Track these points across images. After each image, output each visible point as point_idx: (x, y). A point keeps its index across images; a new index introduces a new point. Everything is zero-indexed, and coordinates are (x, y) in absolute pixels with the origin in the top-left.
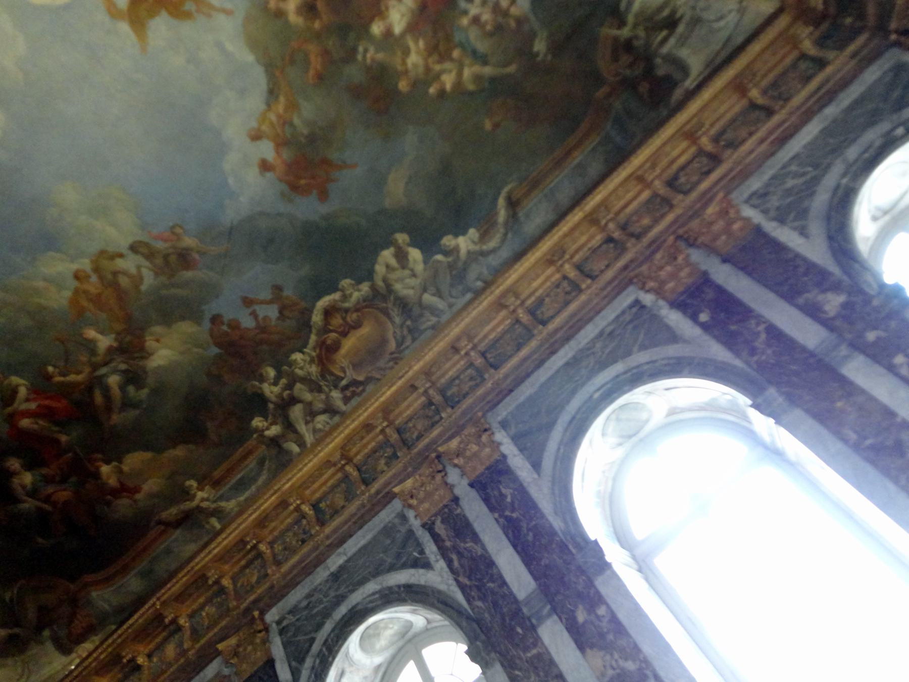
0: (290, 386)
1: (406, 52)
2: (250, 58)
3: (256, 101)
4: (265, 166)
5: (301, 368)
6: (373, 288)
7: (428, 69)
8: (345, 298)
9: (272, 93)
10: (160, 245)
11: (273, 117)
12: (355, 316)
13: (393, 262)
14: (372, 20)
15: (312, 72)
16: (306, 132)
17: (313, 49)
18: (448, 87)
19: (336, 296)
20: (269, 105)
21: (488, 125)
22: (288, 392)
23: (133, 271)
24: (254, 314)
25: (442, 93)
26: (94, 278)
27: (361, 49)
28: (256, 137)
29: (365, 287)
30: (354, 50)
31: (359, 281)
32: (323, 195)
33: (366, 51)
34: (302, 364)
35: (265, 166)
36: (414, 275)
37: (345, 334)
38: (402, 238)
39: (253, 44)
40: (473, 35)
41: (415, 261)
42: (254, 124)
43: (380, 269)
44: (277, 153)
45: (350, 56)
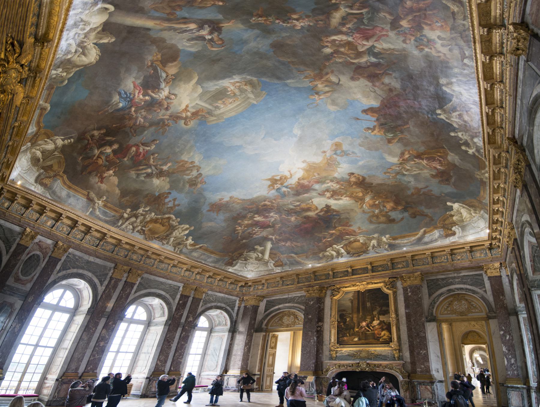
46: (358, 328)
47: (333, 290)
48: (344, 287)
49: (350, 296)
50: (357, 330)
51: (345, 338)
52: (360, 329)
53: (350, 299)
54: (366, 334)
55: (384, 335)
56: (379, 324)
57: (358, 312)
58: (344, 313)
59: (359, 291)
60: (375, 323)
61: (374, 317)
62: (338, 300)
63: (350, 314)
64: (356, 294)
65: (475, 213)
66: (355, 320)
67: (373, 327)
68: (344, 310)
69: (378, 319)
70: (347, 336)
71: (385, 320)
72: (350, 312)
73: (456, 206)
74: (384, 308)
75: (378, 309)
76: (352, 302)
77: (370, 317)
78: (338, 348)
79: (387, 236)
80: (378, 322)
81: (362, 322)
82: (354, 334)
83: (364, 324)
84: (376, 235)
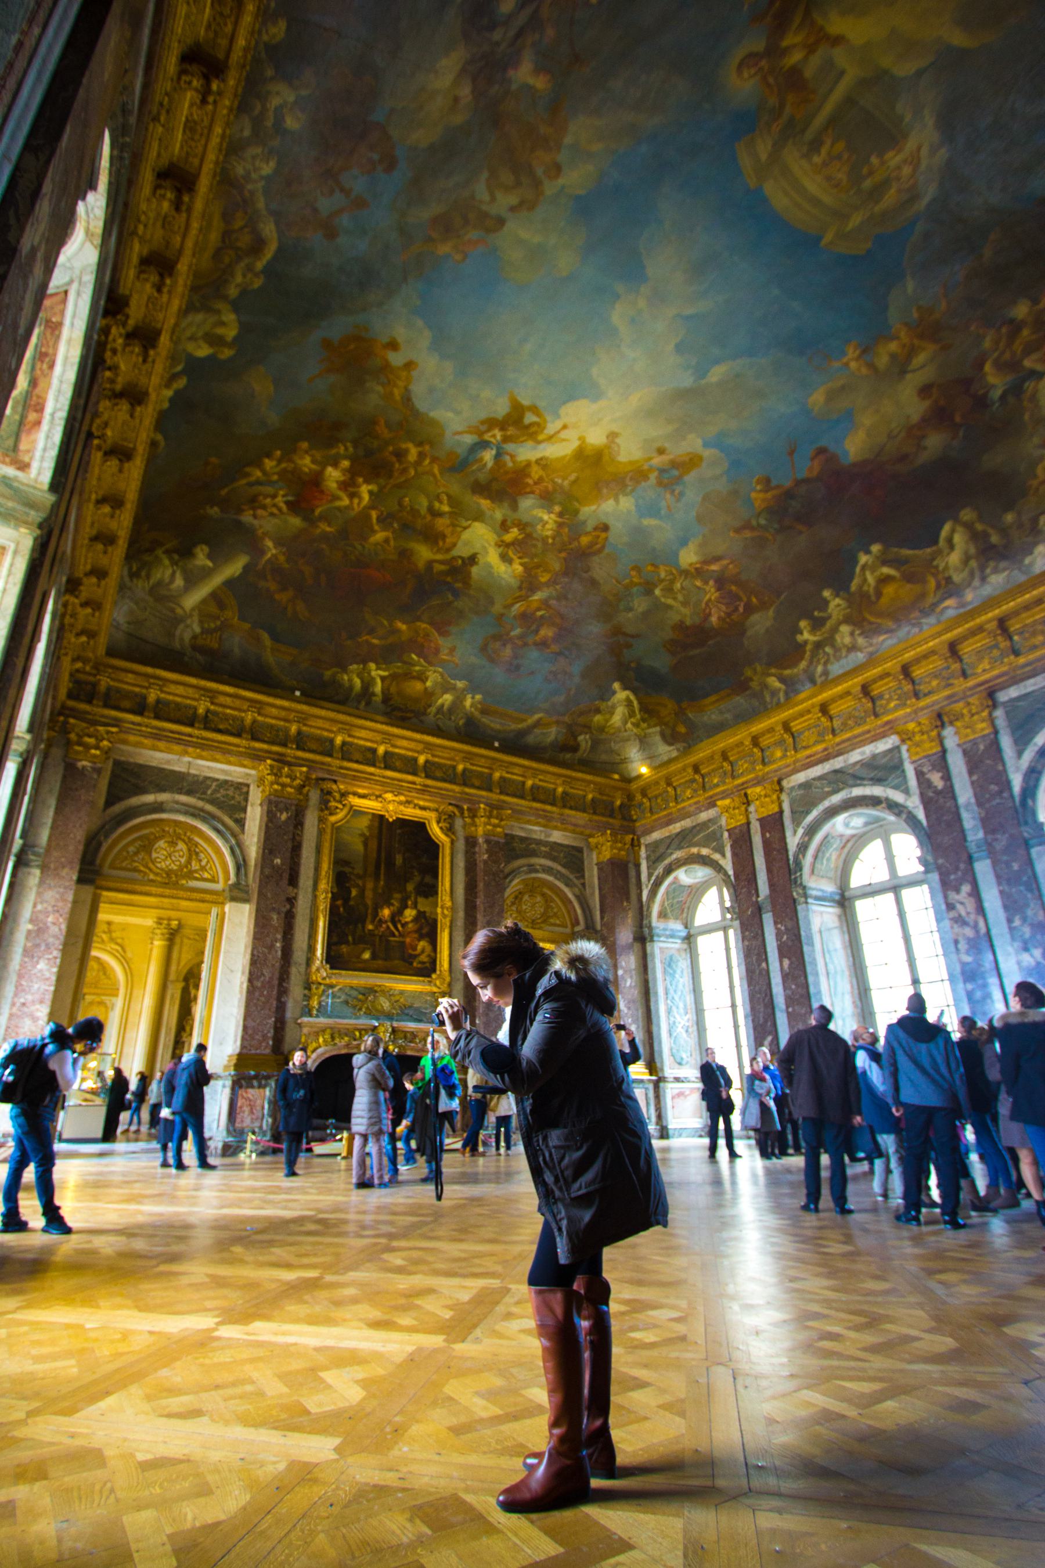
0: (257, 123)
1: (313, 462)
2: (432, 414)
3: (418, 389)
4: (393, 346)
5: (254, 157)
6: (225, 298)
7: (290, 460)
8: (249, 268)
9: (407, 399)
10: (473, 234)
11: (401, 384)
12: (227, 260)
13: (220, 331)
14: (352, 466)
15: (382, 422)
16: (368, 385)
17: (386, 434)
18: (267, 461)
19: (259, 265)
20: (406, 389)
21: (214, 460)
22: (256, 112)
23: (499, 195)
24: (346, 192)
25: (269, 455)
26: (539, 171)
27: (351, 449)
28: (409, 365)
29: (233, 292)
30: (355, 447)
31: (244, 293)
32: (327, 344)
33: (346, 449)
34: (257, 163)
35: (393, 346)
36: (192, 338)
37: (226, 235)
38: (227, 353)
39: (433, 423)
40: (270, 490)
41: (199, 347)
42: (415, 373)
43: (230, 317)
44: (387, 361)
45: (356, 443)
46: (372, 922)
47: (329, 793)
48: (355, 794)
49: (363, 823)
50: (371, 927)
51: (344, 949)
52: (376, 927)
53: (362, 835)
54: (388, 941)
55: (423, 951)
56: (416, 919)
57: (377, 877)
58: (347, 870)
59: (382, 817)
60: (409, 914)
61: (408, 898)
62: (338, 828)
63: (359, 877)
64: (376, 824)
65: (636, 725)
66: (369, 894)
67: (403, 925)
68: (346, 863)
69: (415, 906)
70: (347, 943)
71: (427, 909)
72: (361, 872)
73: (621, 695)
74: (428, 879)
75: (417, 878)
76: (365, 844)
77: (397, 896)
78: (329, 977)
79: (478, 697)
80: (414, 912)
81: (382, 908)
82: (365, 940)
83: (386, 912)
84: (460, 684)
